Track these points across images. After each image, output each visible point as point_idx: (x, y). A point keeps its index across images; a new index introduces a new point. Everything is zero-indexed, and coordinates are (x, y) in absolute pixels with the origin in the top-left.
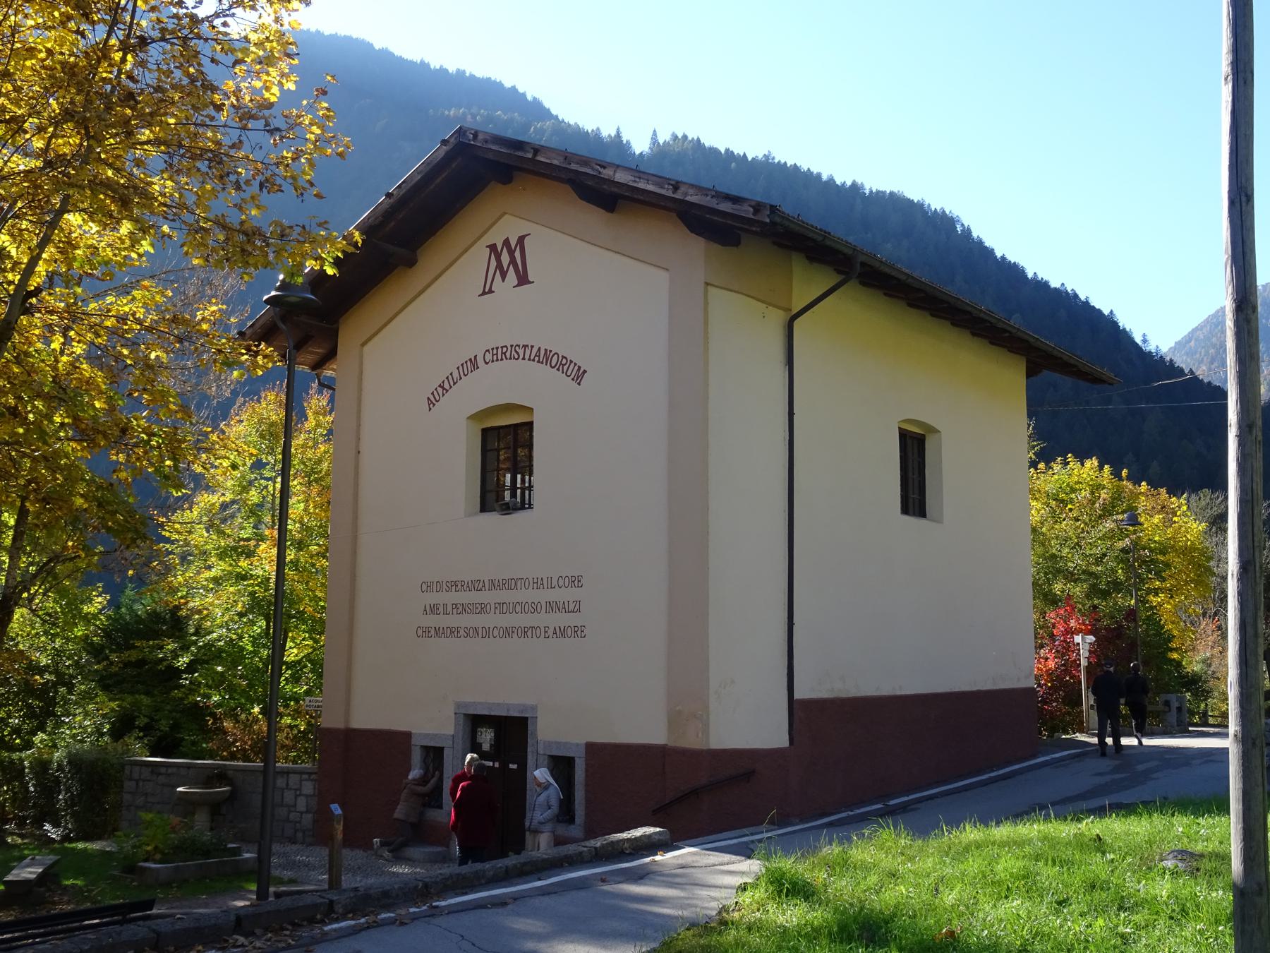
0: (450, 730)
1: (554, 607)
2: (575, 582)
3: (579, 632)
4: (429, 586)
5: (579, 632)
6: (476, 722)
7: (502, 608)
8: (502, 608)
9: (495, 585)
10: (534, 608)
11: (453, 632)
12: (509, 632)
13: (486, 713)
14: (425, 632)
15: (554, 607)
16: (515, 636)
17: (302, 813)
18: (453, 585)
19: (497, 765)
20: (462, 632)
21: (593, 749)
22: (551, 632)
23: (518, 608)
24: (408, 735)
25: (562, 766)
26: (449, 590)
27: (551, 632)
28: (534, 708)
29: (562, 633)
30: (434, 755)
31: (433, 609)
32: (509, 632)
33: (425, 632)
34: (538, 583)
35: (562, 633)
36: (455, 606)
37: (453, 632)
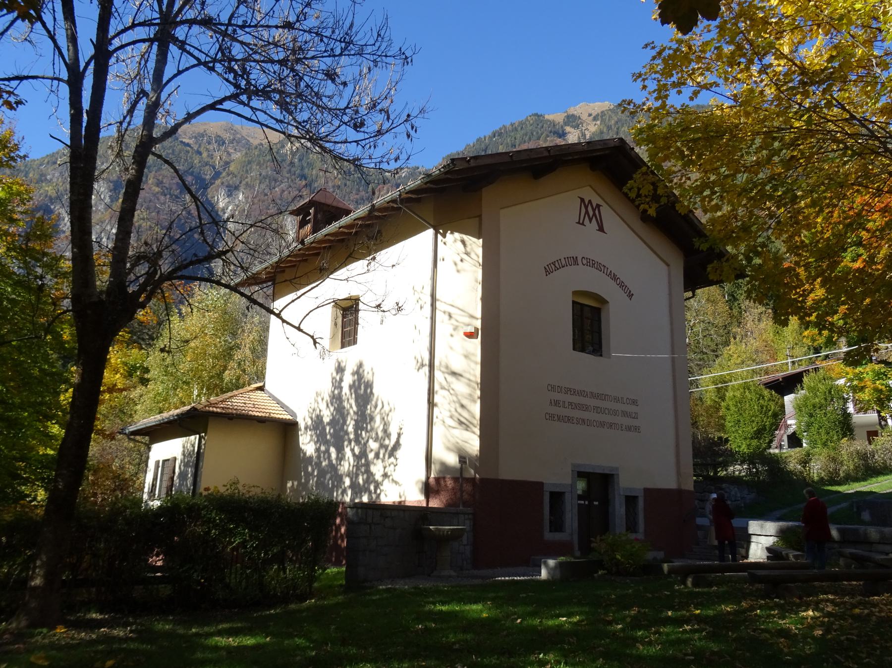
0: (568, 481)
1: (625, 414)
2: (634, 402)
3: (637, 429)
4: (552, 388)
5: (637, 429)
6: (581, 475)
7: (597, 410)
8: (597, 410)
9: (593, 395)
10: (615, 413)
11: (569, 420)
12: (602, 424)
13: (591, 471)
14: (551, 417)
15: (625, 414)
16: (605, 427)
17: (464, 545)
18: (568, 391)
19: (587, 503)
20: (575, 421)
21: (647, 491)
22: (624, 427)
23: (607, 412)
24: (540, 485)
25: (631, 500)
26: (566, 393)
27: (624, 427)
28: (617, 469)
29: (629, 429)
30: (557, 497)
31: (556, 403)
32: (602, 424)
33: (551, 417)
34: (617, 400)
35: (629, 429)
36: (570, 404)
37: (569, 420)
